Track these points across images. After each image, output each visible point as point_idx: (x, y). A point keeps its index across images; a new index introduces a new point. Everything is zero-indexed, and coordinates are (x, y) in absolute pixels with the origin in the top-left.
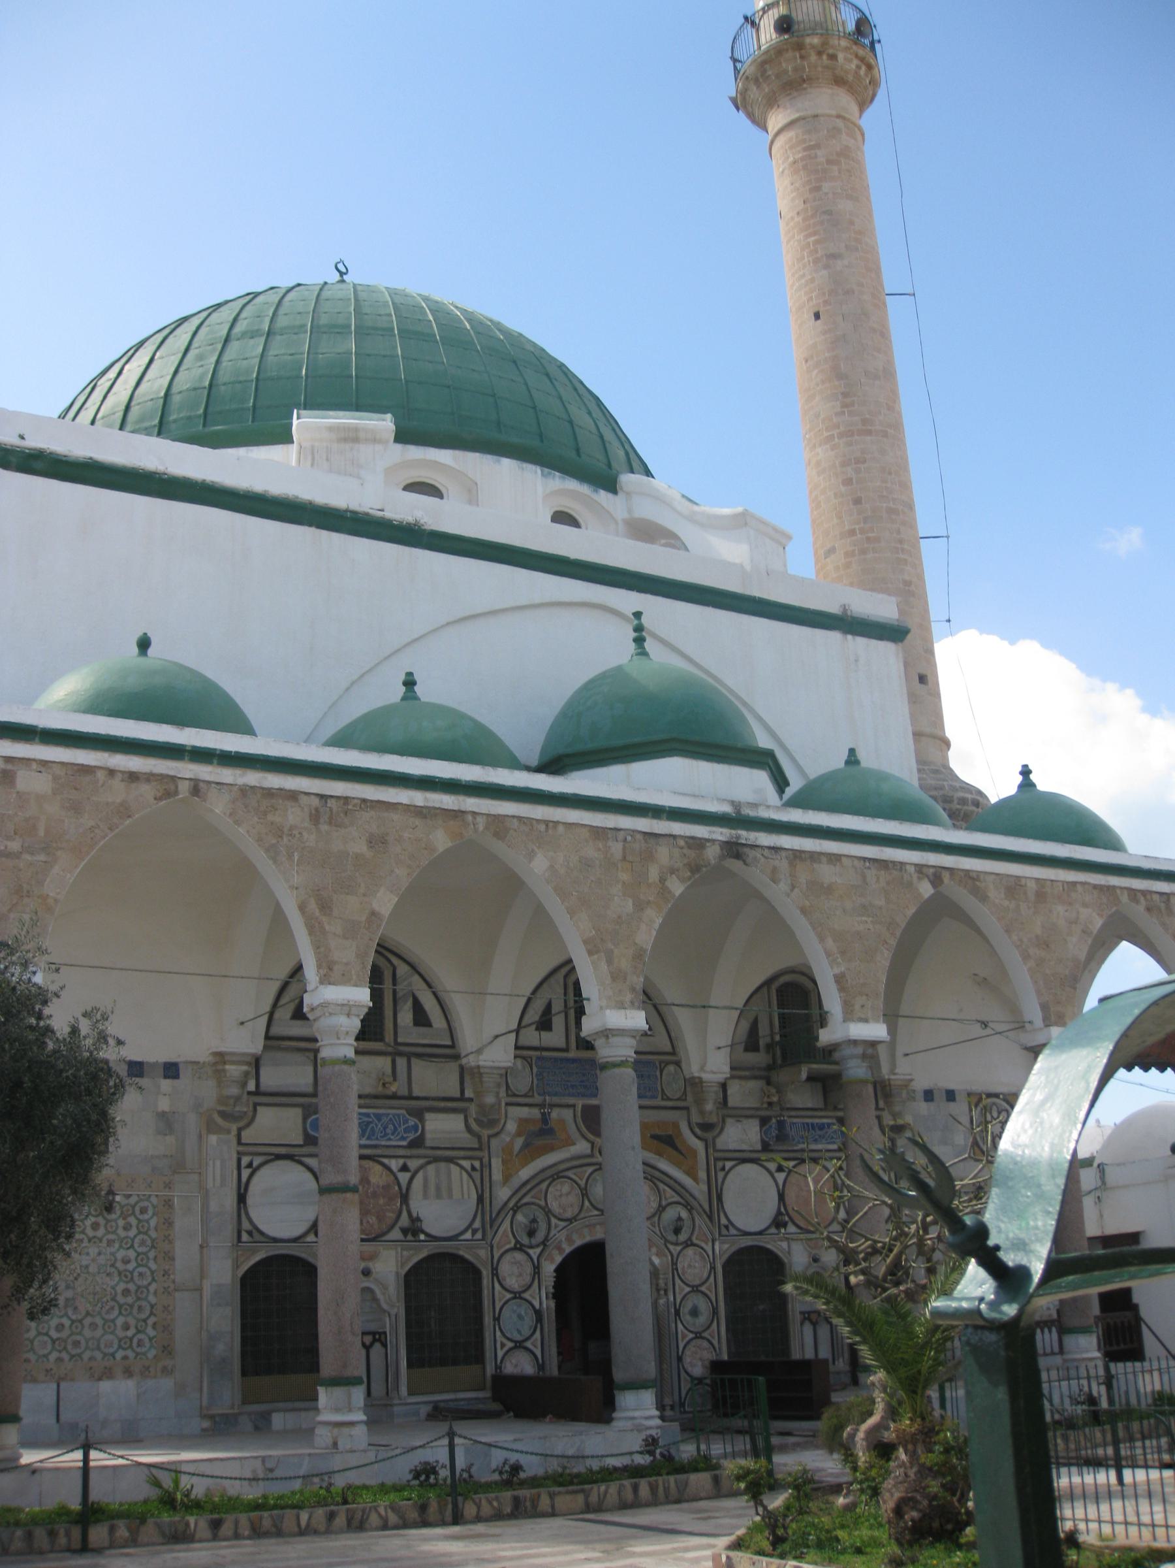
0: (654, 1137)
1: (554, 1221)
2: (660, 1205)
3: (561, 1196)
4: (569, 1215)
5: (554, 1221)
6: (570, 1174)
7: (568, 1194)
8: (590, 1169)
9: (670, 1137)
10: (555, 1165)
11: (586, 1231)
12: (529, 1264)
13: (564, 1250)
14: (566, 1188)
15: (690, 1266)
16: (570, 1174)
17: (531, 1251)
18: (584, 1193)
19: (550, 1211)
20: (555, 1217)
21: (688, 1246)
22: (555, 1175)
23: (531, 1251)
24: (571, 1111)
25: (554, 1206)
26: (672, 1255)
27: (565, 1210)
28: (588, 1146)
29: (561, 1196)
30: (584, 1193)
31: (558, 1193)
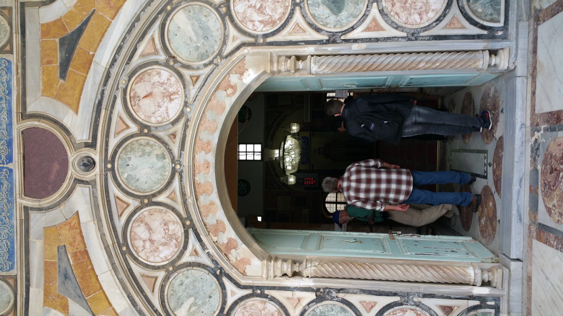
0: (63, 74)
1: (187, 258)
2: (166, 65)
3: (152, 241)
4: (178, 230)
5: (187, 258)
6: (120, 224)
7: (150, 229)
8: (114, 190)
9: (62, 42)
10: (107, 248)
11: (202, 199)
12: (250, 302)
13: (230, 240)
14: (140, 231)
15: (261, 10)
16: (120, 224)
17: (230, 301)
18: (148, 200)
19: (173, 263)
20: (180, 257)
21: (229, 13)
22: (122, 248)
23: (230, 301)
24: (33, 215)
25: (166, 254)
26: (243, 45)
27: (171, 237)
28: (79, 189)
29: (152, 241)
30: (148, 200)
31: (148, 244)
